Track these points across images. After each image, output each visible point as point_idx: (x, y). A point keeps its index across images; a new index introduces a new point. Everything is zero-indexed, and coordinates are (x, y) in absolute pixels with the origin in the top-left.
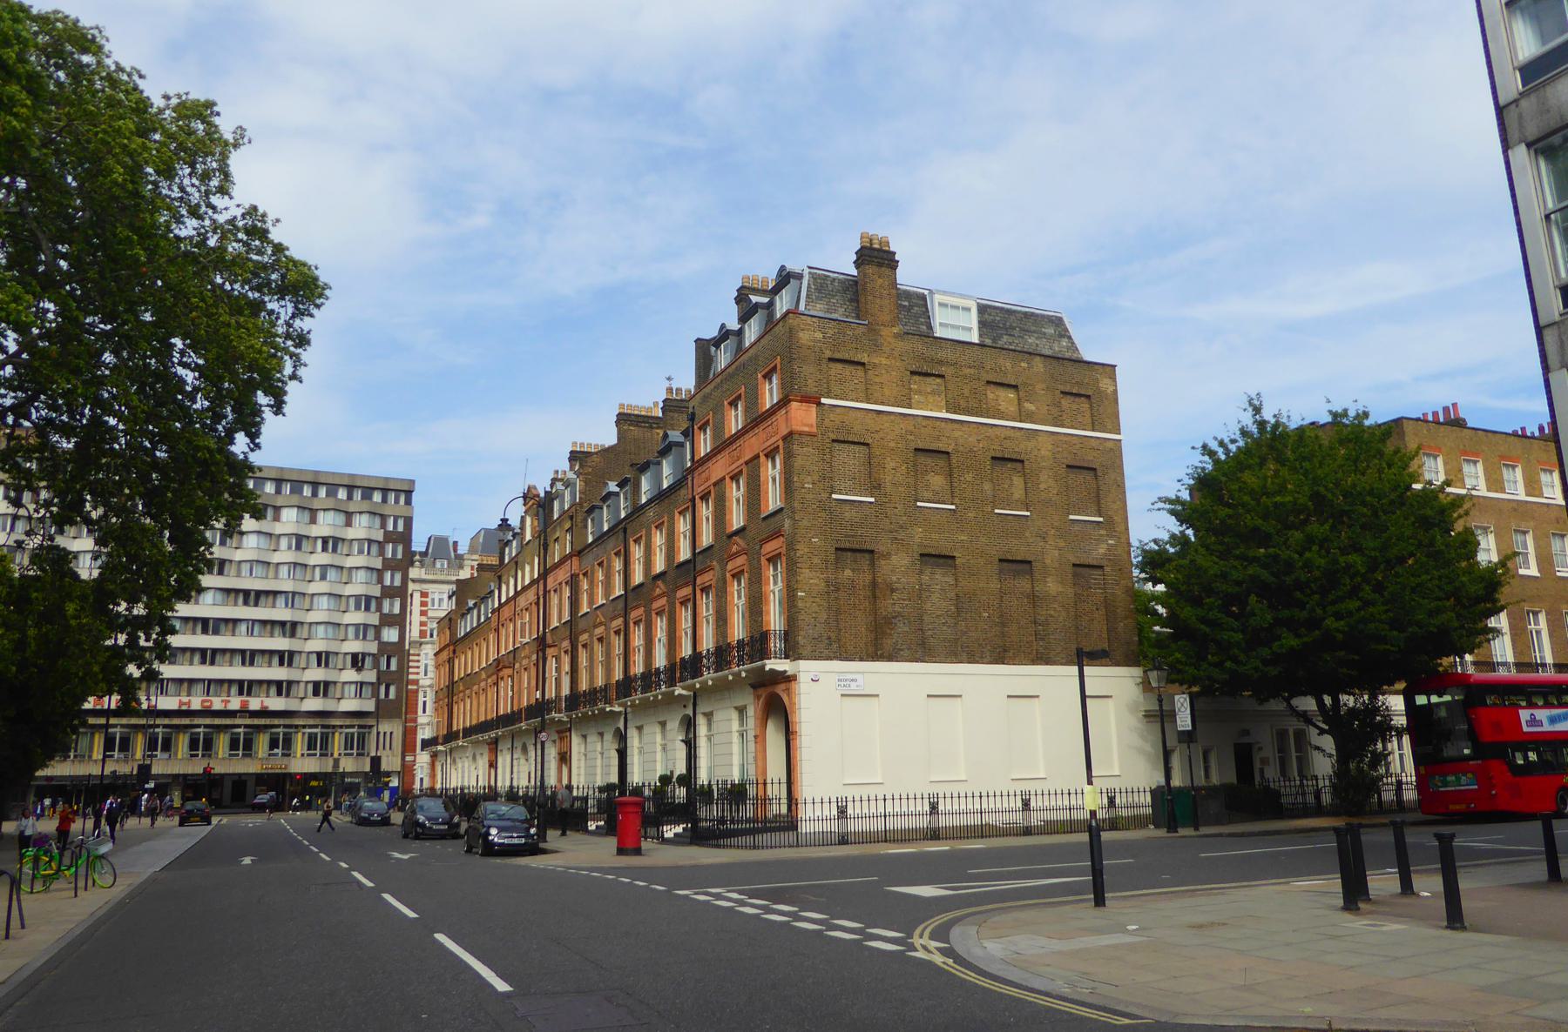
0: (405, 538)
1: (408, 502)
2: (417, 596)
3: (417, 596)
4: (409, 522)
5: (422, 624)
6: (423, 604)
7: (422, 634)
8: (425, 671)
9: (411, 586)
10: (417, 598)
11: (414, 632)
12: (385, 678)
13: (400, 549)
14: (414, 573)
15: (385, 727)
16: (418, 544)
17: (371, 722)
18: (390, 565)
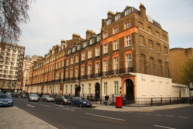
0: (23, 55)
1: (24, 50)
2: (24, 64)
3: (24, 64)
4: (24, 53)
5: (25, 68)
6: (25, 65)
7: (25, 69)
8: (26, 74)
9: (24, 62)
10: (24, 64)
11: (24, 69)
12: (19, 76)
13: (22, 57)
14: (24, 60)
15: (18, 83)
16: (25, 57)
17: (16, 82)
18: (20, 59)
